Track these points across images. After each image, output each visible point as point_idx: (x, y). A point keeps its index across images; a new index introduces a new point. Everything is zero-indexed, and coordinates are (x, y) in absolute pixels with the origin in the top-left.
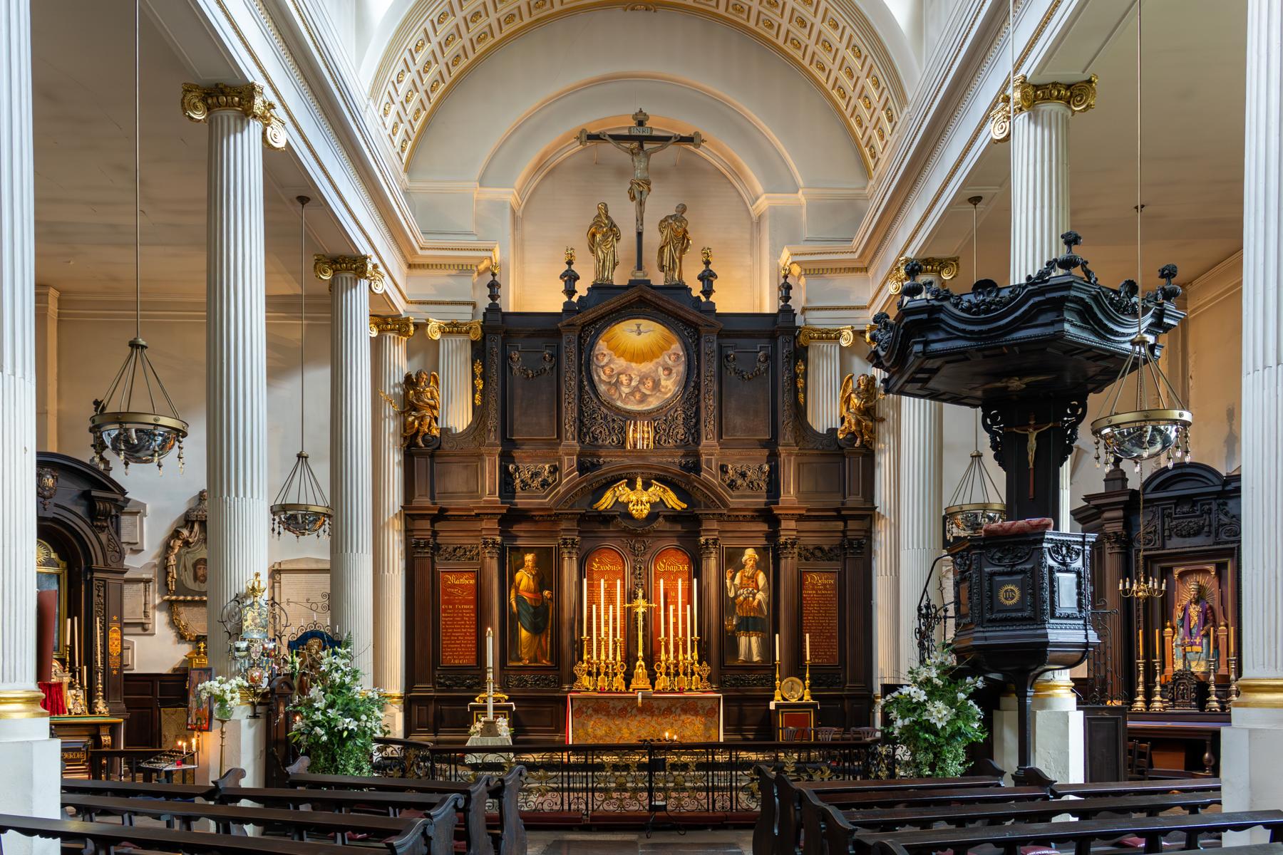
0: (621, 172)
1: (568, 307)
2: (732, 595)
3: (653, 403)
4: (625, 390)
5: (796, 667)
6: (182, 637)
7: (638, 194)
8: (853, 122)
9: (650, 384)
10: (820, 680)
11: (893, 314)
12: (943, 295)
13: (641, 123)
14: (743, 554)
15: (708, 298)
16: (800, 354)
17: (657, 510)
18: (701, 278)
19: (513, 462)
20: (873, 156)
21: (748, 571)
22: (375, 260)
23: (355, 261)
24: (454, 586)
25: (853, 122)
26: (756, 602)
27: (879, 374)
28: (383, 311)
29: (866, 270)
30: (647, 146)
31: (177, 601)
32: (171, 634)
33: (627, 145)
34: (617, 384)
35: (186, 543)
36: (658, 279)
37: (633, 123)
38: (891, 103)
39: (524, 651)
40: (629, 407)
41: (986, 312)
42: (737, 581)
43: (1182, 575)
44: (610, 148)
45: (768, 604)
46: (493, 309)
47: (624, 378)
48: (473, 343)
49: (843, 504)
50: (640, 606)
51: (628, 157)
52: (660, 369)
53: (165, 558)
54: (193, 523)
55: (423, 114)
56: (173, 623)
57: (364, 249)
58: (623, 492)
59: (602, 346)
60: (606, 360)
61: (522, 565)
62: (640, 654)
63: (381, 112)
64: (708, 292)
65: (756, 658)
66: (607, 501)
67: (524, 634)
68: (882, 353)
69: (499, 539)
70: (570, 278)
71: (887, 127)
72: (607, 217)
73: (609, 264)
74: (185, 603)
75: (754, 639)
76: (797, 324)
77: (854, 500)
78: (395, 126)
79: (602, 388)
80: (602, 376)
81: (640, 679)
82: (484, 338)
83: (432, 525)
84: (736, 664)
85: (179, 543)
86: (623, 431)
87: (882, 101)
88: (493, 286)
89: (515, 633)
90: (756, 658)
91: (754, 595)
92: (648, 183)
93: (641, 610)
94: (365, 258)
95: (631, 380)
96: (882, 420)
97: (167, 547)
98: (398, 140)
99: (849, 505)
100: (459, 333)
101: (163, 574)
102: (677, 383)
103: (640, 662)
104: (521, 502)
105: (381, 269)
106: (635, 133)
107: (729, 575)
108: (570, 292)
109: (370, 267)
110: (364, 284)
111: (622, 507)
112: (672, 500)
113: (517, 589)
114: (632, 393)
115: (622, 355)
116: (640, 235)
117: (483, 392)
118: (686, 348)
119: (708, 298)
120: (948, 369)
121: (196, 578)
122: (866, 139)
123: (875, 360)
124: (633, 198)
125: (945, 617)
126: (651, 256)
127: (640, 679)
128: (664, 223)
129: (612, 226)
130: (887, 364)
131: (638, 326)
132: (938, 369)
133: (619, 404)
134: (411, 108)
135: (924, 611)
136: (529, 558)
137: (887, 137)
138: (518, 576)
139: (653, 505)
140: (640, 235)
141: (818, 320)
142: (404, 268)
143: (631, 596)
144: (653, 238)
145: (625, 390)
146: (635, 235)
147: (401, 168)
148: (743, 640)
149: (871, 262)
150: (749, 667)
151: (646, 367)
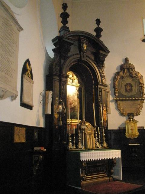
6: (122, 114)
31: (119, 100)
32: (117, 113)
35: (123, 77)
53: (114, 83)
54: (124, 69)
56: (118, 108)
74: (123, 100)
85: (119, 77)
97: (115, 78)
101: (113, 89)
121: (126, 91)
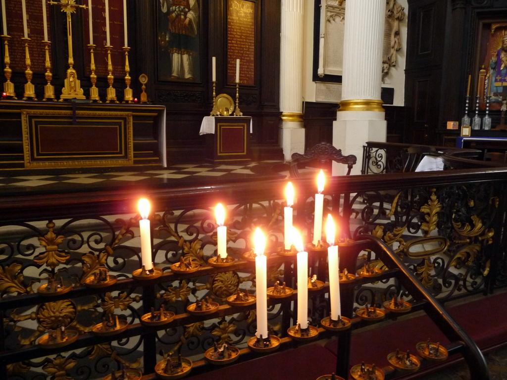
5: (225, 85)
26: (187, 21)
43: (497, 29)
62: (71, 60)
65: (187, 76)
75: (185, 57)
81: (73, 89)
84: (169, 79)
90: (187, 76)
91: (186, 13)
103: (71, 70)
127: (73, 89)
148: (176, 57)
150: (181, 83)
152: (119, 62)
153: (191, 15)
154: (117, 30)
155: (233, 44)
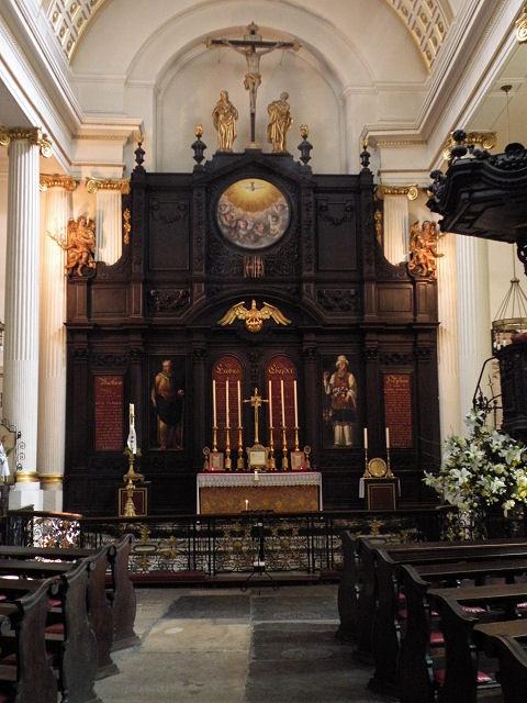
0: (238, 69)
1: (197, 169)
2: (328, 392)
3: (265, 243)
4: (242, 232)
5: (377, 450)
7: (252, 83)
8: (414, 33)
9: (261, 228)
10: (396, 460)
11: (445, 170)
12: (485, 155)
13: (253, 33)
14: (336, 360)
15: (306, 163)
16: (379, 205)
17: (268, 322)
18: (300, 148)
19: (154, 288)
20: (430, 58)
21: (341, 373)
22: (45, 131)
23: (28, 132)
24: (105, 386)
25: (414, 33)
27: (438, 217)
28: (51, 171)
29: (426, 142)
30: (257, 50)
33: (243, 49)
34: (237, 228)
36: (268, 149)
37: (248, 33)
38: (441, 19)
39: (162, 439)
40: (245, 246)
41: (514, 167)
42: (332, 381)
44: (230, 51)
45: (357, 400)
46: (139, 170)
47: (241, 224)
48: (123, 196)
49: (415, 320)
50: (256, 401)
51: (243, 57)
52: (270, 217)
55: (85, 22)
57: (36, 122)
58: (239, 312)
59: (224, 198)
60: (227, 210)
61: (161, 369)
63: (51, 18)
64: (306, 158)
65: (348, 443)
66: (229, 319)
67: (162, 424)
68: (438, 201)
69: (141, 349)
70: (199, 147)
71: (439, 36)
72: (228, 102)
73: (229, 137)
75: (346, 427)
76: (375, 182)
77: (422, 318)
78: (63, 30)
79: (225, 231)
80: (224, 221)
82: (131, 192)
83: (88, 337)
86: (242, 265)
87: (435, 17)
88: (140, 153)
89: (156, 424)
90: (348, 443)
92: (259, 77)
93: (257, 405)
94: (37, 129)
95: (247, 224)
96: (442, 255)
98: (64, 40)
99: (419, 320)
100: (113, 188)
102: (282, 227)
104: (159, 319)
105: (49, 138)
106: (249, 39)
107: (325, 377)
108: (199, 158)
109: (40, 136)
110: (35, 149)
111: (240, 322)
112: (280, 319)
113: (157, 389)
114: (248, 235)
115: (240, 206)
116: (253, 115)
117: (130, 234)
118: (289, 201)
119: (306, 163)
120: (490, 213)
122: (424, 45)
123: (432, 206)
124: (248, 88)
125: (495, 408)
126: (261, 131)
128: (271, 107)
129: (232, 109)
130: (441, 209)
131: (252, 184)
132: (482, 212)
133: (238, 243)
134: (74, 17)
135: (478, 403)
136: (166, 363)
137: (439, 44)
138: (158, 378)
139: (264, 321)
140: (253, 115)
141: (388, 180)
142: (70, 138)
143: (247, 394)
144: (262, 115)
145: (242, 232)
146: (249, 118)
147: (67, 63)
148: (338, 429)
149: (430, 136)
150: (343, 450)
151: (259, 215)
152: (290, 437)
153: (350, 393)
154: (290, 412)
155: (389, 412)
